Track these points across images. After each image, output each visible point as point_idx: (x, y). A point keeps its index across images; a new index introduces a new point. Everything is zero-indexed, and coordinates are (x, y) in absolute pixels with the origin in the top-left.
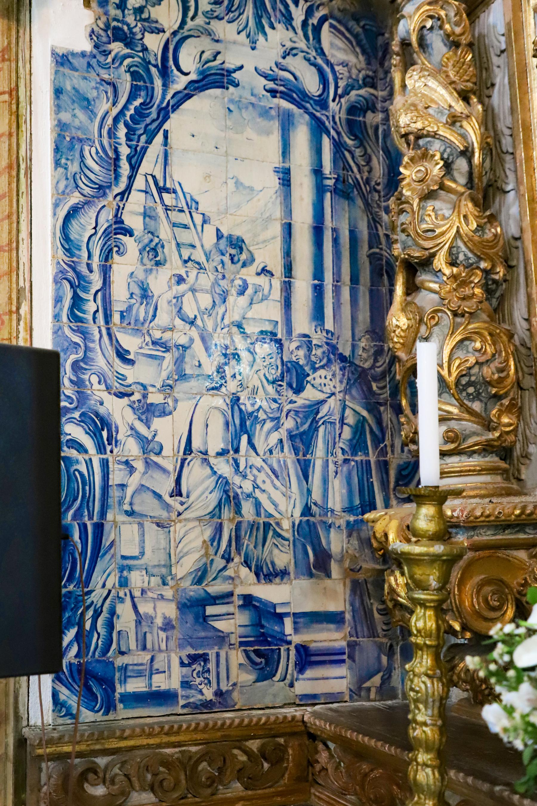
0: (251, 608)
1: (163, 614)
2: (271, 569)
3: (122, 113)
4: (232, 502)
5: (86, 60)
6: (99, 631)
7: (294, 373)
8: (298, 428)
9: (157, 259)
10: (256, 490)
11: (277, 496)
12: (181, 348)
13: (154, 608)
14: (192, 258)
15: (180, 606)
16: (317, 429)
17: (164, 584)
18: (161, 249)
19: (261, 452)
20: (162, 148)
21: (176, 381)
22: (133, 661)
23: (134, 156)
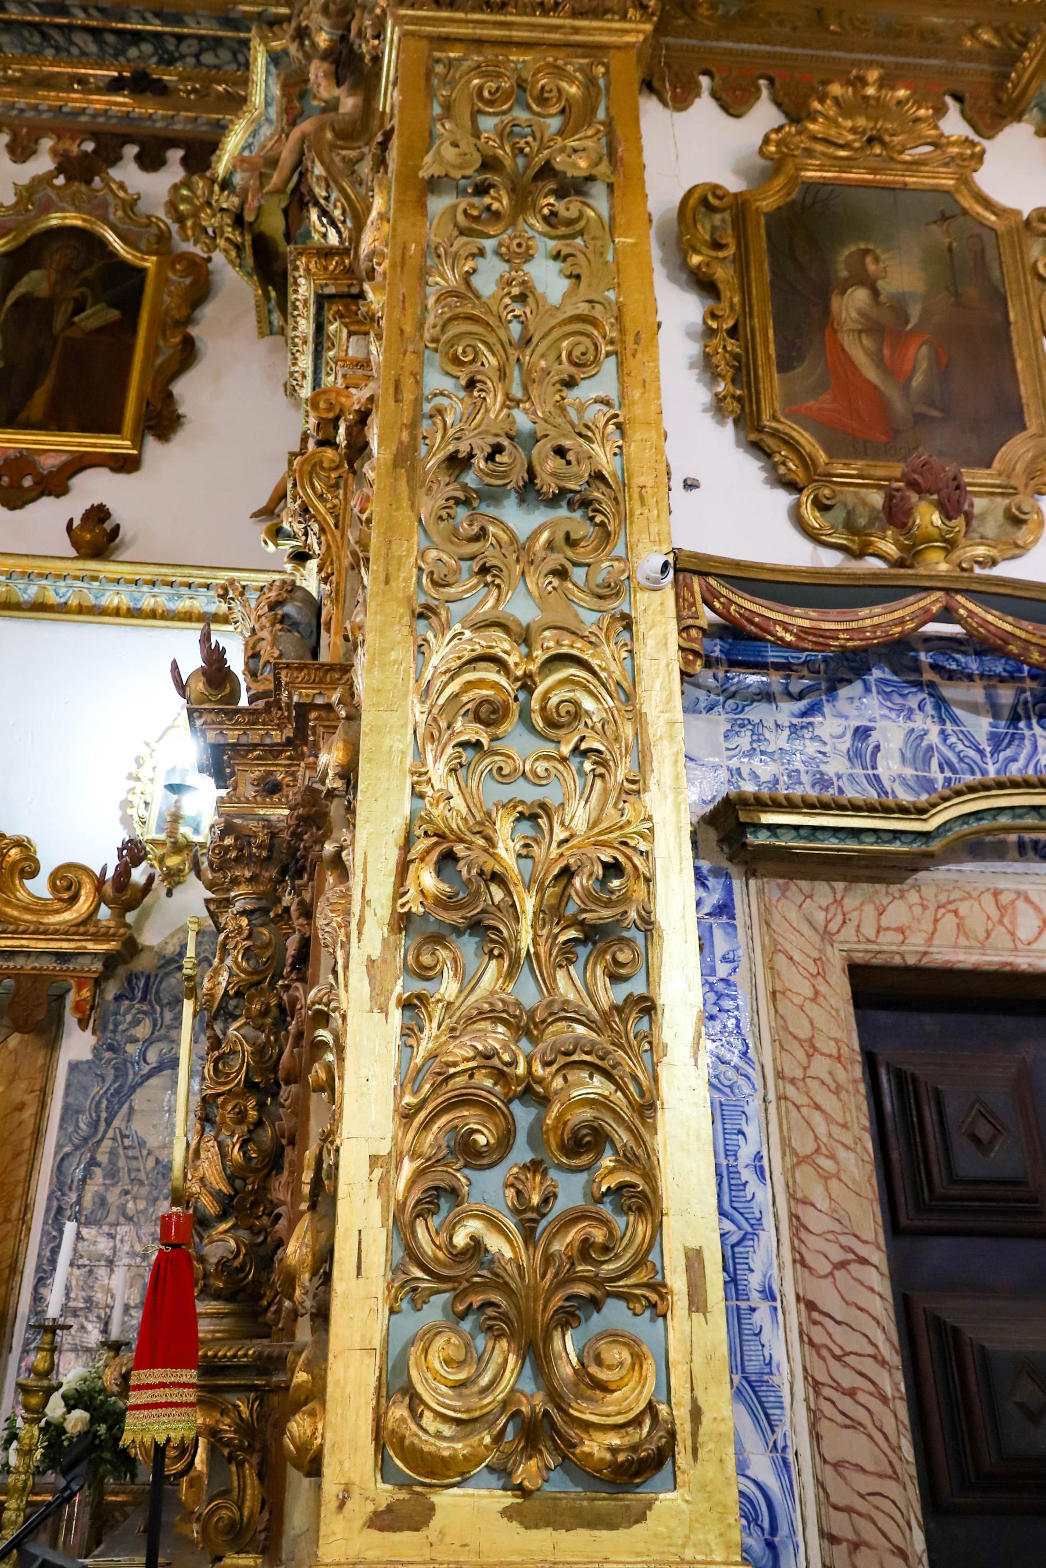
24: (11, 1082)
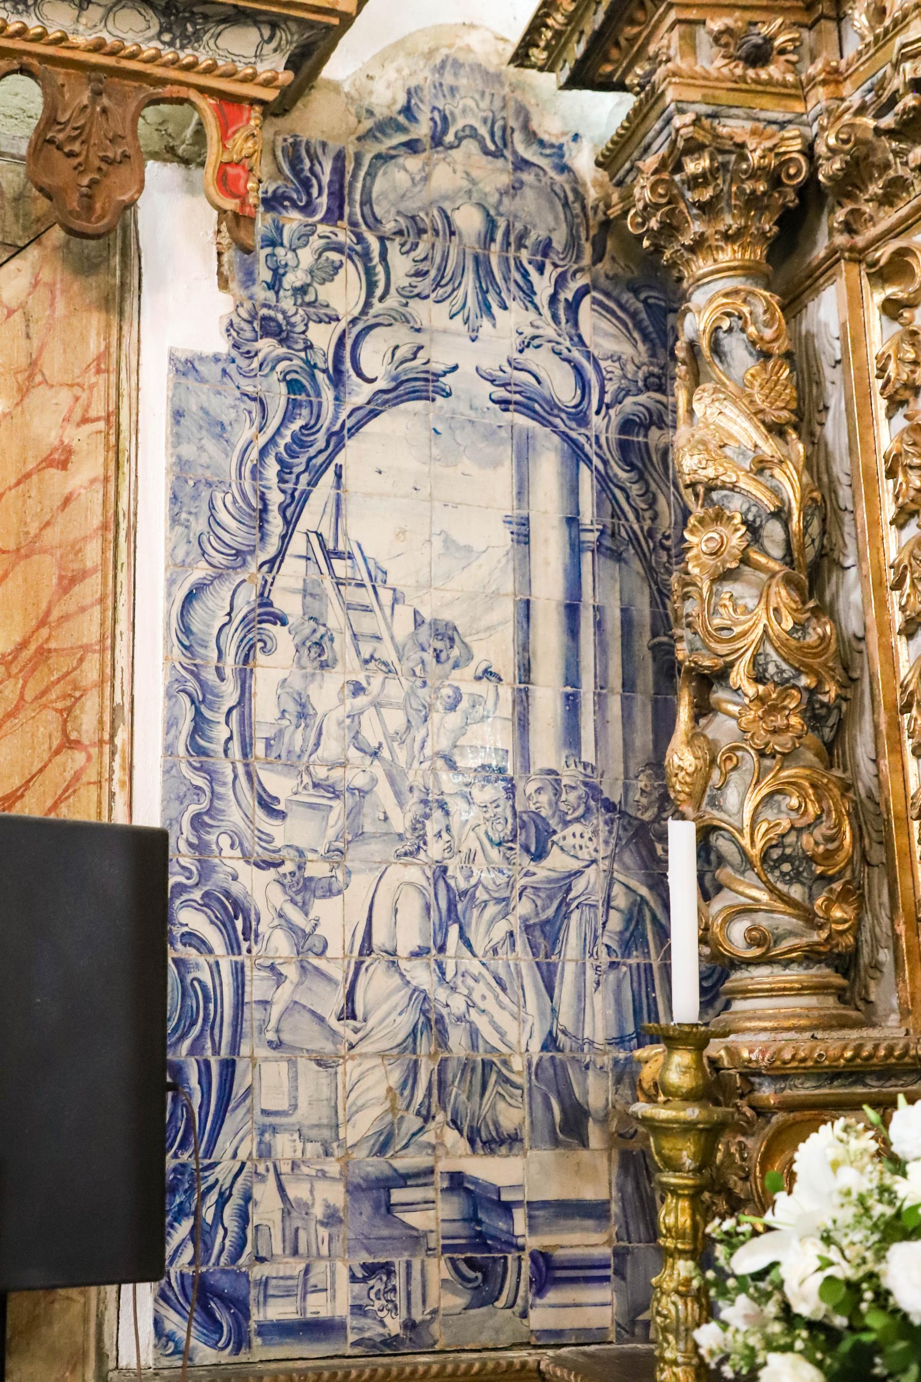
0: (463, 1194)
1: (325, 1200)
2: (494, 1134)
3: (272, 441)
4: (434, 1029)
5: (221, 365)
6: (226, 1225)
7: (533, 830)
8: (537, 914)
9: (323, 658)
10: (471, 1009)
11: (504, 1020)
12: (356, 792)
13: (311, 1192)
14: (376, 656)
15: (351, 1188)
16: (567, 916)
17: (327, 1154)
18: (328, 643)
19: (479, 951)
20: (334, 492)
21: (349, 842)
22: (278, 1272)
23: (289, 505)
24: (24, 392)
